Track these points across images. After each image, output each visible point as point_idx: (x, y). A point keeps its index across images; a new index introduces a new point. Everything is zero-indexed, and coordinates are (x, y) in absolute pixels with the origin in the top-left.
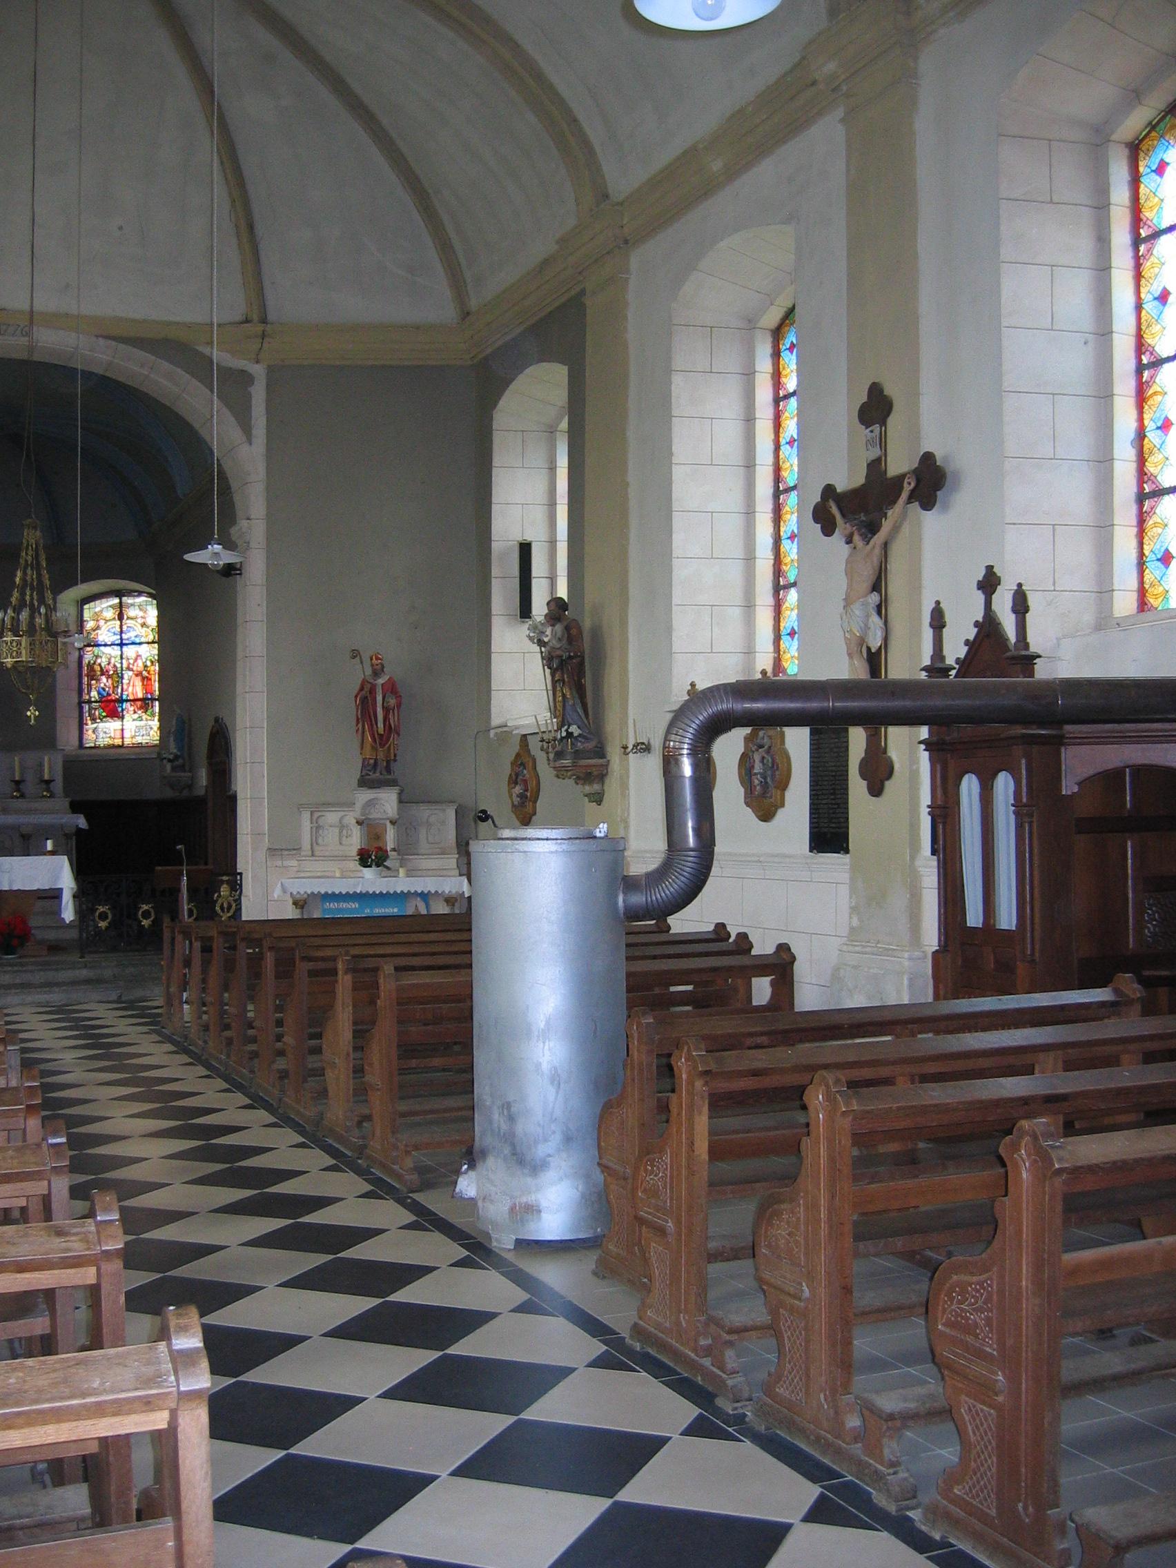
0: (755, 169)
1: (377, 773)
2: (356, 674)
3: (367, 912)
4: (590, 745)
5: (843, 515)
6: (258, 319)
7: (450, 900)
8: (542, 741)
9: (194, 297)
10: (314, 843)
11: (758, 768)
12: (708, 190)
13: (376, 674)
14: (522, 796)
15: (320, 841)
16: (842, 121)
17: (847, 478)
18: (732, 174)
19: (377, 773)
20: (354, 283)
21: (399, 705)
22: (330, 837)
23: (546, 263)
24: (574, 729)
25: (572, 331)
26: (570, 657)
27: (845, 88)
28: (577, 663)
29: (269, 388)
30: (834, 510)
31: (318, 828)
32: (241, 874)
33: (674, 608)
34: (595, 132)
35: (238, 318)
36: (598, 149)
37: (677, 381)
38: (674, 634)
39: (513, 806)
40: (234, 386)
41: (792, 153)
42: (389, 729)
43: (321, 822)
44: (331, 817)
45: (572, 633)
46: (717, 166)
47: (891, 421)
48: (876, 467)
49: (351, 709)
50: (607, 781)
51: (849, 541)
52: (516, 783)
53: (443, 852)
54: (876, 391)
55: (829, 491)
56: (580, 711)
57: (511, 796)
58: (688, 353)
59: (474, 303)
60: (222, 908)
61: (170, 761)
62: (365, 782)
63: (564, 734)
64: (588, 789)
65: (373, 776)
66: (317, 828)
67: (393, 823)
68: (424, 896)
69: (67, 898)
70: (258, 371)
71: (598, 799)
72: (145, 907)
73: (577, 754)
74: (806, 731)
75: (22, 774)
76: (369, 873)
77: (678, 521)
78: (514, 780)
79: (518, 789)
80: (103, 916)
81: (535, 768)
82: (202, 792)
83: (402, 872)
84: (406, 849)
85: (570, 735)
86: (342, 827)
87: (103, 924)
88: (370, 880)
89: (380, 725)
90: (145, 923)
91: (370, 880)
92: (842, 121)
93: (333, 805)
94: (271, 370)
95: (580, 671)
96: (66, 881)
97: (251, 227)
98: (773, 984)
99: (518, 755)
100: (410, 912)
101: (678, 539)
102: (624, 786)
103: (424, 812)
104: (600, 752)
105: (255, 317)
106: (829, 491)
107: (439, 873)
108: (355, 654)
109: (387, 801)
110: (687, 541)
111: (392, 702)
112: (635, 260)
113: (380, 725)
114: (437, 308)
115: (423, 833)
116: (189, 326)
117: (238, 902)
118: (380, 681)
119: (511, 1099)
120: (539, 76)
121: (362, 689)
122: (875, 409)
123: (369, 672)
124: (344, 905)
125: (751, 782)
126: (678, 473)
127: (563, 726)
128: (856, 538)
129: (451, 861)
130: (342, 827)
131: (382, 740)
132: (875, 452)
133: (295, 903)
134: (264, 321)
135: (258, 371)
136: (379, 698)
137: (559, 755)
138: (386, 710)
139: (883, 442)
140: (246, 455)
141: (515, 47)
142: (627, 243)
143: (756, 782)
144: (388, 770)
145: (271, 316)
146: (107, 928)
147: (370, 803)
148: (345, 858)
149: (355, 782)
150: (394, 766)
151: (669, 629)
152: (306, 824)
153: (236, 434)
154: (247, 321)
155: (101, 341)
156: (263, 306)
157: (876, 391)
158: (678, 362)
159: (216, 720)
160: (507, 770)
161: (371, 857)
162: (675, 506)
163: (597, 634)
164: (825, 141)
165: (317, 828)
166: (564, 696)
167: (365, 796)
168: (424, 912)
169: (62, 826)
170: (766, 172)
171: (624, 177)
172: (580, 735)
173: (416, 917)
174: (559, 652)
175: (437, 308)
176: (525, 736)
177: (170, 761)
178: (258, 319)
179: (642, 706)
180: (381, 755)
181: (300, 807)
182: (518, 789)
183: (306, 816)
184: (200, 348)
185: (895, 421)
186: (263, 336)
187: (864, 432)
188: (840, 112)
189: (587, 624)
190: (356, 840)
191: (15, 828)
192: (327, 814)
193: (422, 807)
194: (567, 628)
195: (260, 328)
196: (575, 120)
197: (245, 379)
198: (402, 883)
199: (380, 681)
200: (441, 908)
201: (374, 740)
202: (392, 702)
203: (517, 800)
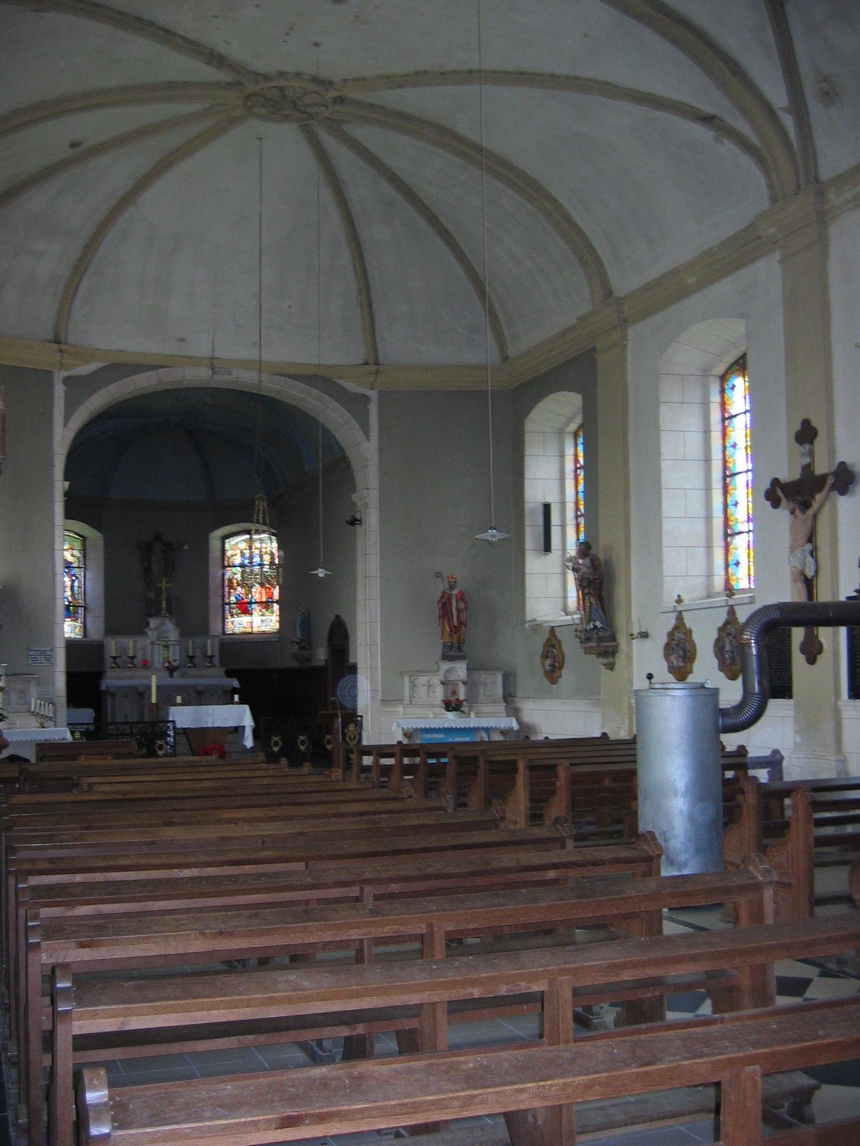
0: (717, 284)
1: (453, 651)
2: (440, 587)
3: (450, 740)
4: (607, 634)
5: (786, 497)
6: (373, 362)
7: (503, 732)
8: (576, 631)
9: (337, 351)
10: (412, 695)
11: (728, 647)
12: (685, 293)
13: (452, 587)
14: (552, 666)
15: (415, 694)
16: (779, 262)
17: (788, 473)
18: (702, 285)
19: (453, 651)
20: (430, 340)
21: (466, 608)
22: (422, 691)
23: (570, 329)
24: (598, 624)
25: (590, 373)
26: (595, 579)
27: (781, 242)
28: (598, 580)
29: (380, 406)
30: (780, 493)
31: (415, 686)
32: (361, 716)
33: (664, 549)
34: (604, 254)
35: (361, 361)
36: (605, 263)
37: (663, 408)
38: (664, 565)
39: (545, 672)
40: (356, 404)
41: (745, 275)
42: (461, 623)
43: (416, 682)
44: (422, 680)
45: (595, 564)
46: (691, 280)
47: (817, 442)
48: (807, 469)
49: (436, 612)
50: (617, 655)
51: (793, 512)
52: (547, 657)
53: (494, 702)
54: (806, 423)
55: (775, 482)
56: (600, 611)
57: (543, 665)
58: (669, 392)
59: (511, 352)
60: (350, 738)
61: (298, 643)
62: (446, 657)
63: (592, 627)
64: (605, 661)
65: (452, 653)
66: (413, 686)
67: (464, 683)
68: (487, 730)
69: (248, 733)
70: (373, 394)
71: (611, 667)
72: (302, 738)
73: (600, 639)
74: (843, 631)
75: (212, 652)
76: (451, 715)
77: (665, 495)
78: (545, 656)
79: (548, 662)
80: (276, 744)
81: (560, 648)
82: (322, 663)
83: (472, 714)
84: (472, 699)
85: (595, 627)
86: (429, 686)
87: (276, 749)
88: (451, 719)
89: (455, 620)
90: (302, 748)
91: (451, 719)
92: (779, 262)
93: (424, 672)
94: (382, 395)
95: (601, 585)
96: (248, 722)
97: (370, 306)
98: (769, 773)
99: (549, 640)
100: (478, 740)
101: (665, 506)
102: (630, 658)
103: (483, 676)
104: (613, 638)
105: (372, 361)
106: (775, 482)
107: (492, 715)
108: (439, 575)
109: (460, 670)
110: (671, 507)
111: (462, 605)
112: (631, 333)
113: (455, 620)
114: (488, 353)
115: (481, 690)
116: (330, 367)
117: (360, 735)
118: (455, 592)
119: (665, 829)
120: (568, 218)
121: (442, 597)
122: (806, 434)
123: (447, 586)
124: (436, 736)
125: (723, 655)
126: (665, 465)
127: (590, 621)
128: (797, 512)
129: (502, 707)
130: (429, 686)
131: (455, 630)
132: (807, 460)
133: (405, 735)
134: (377, 363)
135: (373, 394)
136: (454, 603)
137: (588, 640)
138: (459, 611)
139: (811, 454)
140: (366, 450)
141: (554, 201)
142: (624, 323)
143: (727, 656)
144: (460, 649)
145: (381, 360)
146: (279, 751)
147: (449, 671)
148: (433, 706)
149: (439, 657)
150: (464, 647)
151: (660, 562)
152: (407, 684)
153: (360, 435)
154: (366, 364)
155: (277, 377)
156: (376, 352)
157: (806, 423)
158: (663, 397)
159: (337, 617)
160: (540, 649)
161: (452, 705)
162: (664, 486)
163: (609, 563)
164: (767, 272)
165: (413, 686)
166: (590, 603)
167: (445, 666)
168: (486, 739)
169: (222, 687)
170: (725, 287)
171: (624, 283)
172: (602, 628)
173: (482, 742)
174: (588, 576)
175: (488, 353)
176: (553, 627)
177: (298, 643)
178: (373, 362)
179: (644, 612)
180: (455, 641)
181: (402, 673)
182: (548, 662)
183: (406, 679)
184: (337, 381)
185: (820, 443)
186: (377, 373)
187: (799, 449)
188: (777, 256)
189: (602, 557)
190: (439, 693)
191: (194, 687)
192: (421, 678)
193: (481, 672)
194: (592, 560)
195: (373, 368)
196: (591, 246)
197: (366, 400)
198: (472, 722)
199: (455, 592)
200: (497, 737)
201: (450, 628)
202: (462, 605)
203: (548, 668)
